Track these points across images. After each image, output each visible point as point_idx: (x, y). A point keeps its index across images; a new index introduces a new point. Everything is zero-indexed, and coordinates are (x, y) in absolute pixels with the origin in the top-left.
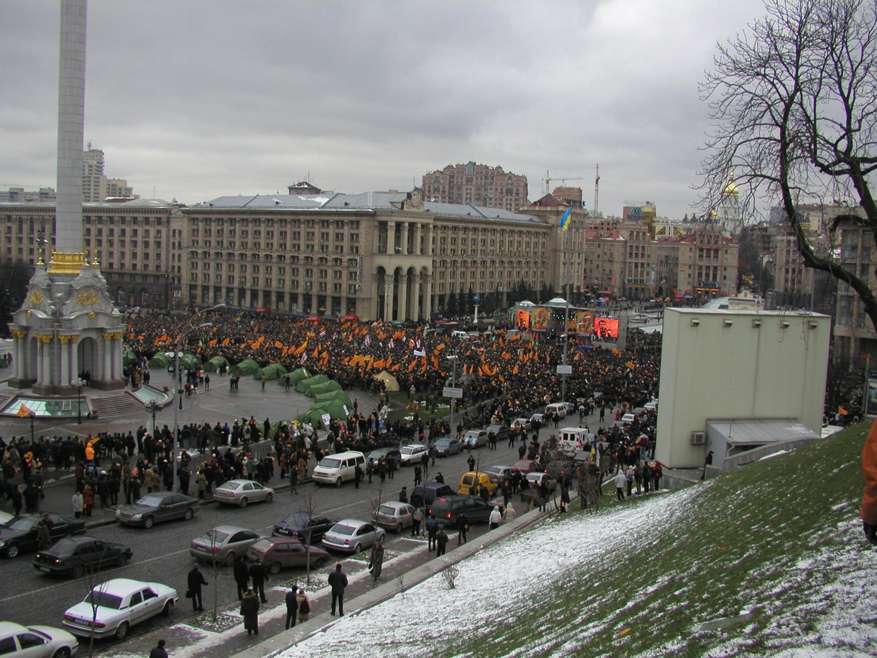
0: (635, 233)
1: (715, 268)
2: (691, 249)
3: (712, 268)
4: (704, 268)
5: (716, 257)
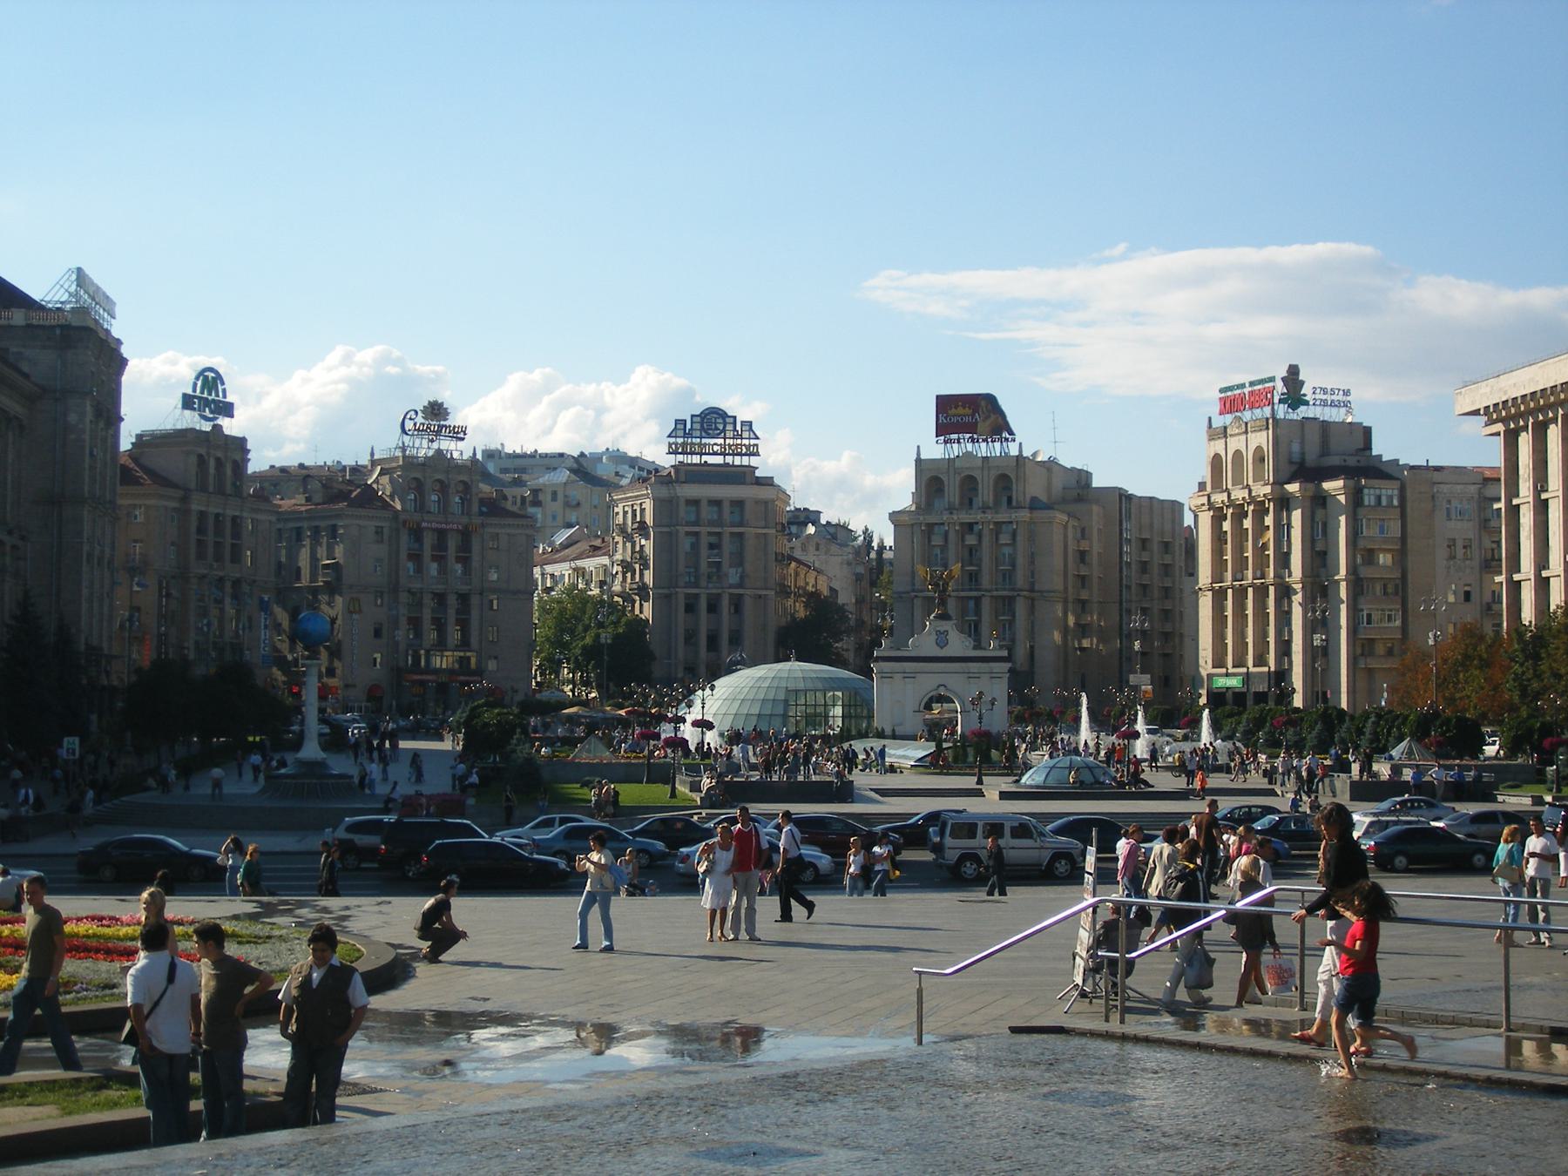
0: (212, 463)
1: (464, 598)
2: (379, 531)
3: (452, 601)
4: (428, 601)
5: (465, 560)
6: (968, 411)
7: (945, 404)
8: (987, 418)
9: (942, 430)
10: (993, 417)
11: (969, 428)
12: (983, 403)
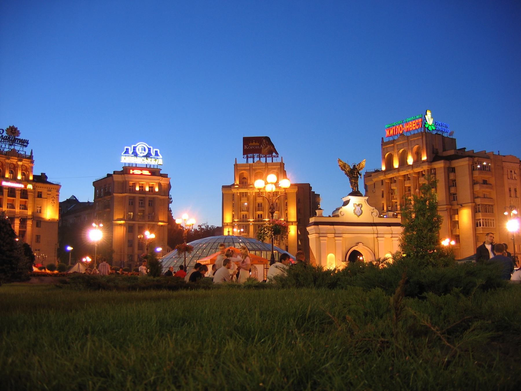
6: (257, 144)
7: (247, 141)
8: (266, 147)
9: (246, 152)
10: (268, 146)
11: (258, 151)
12: (264, 141)
